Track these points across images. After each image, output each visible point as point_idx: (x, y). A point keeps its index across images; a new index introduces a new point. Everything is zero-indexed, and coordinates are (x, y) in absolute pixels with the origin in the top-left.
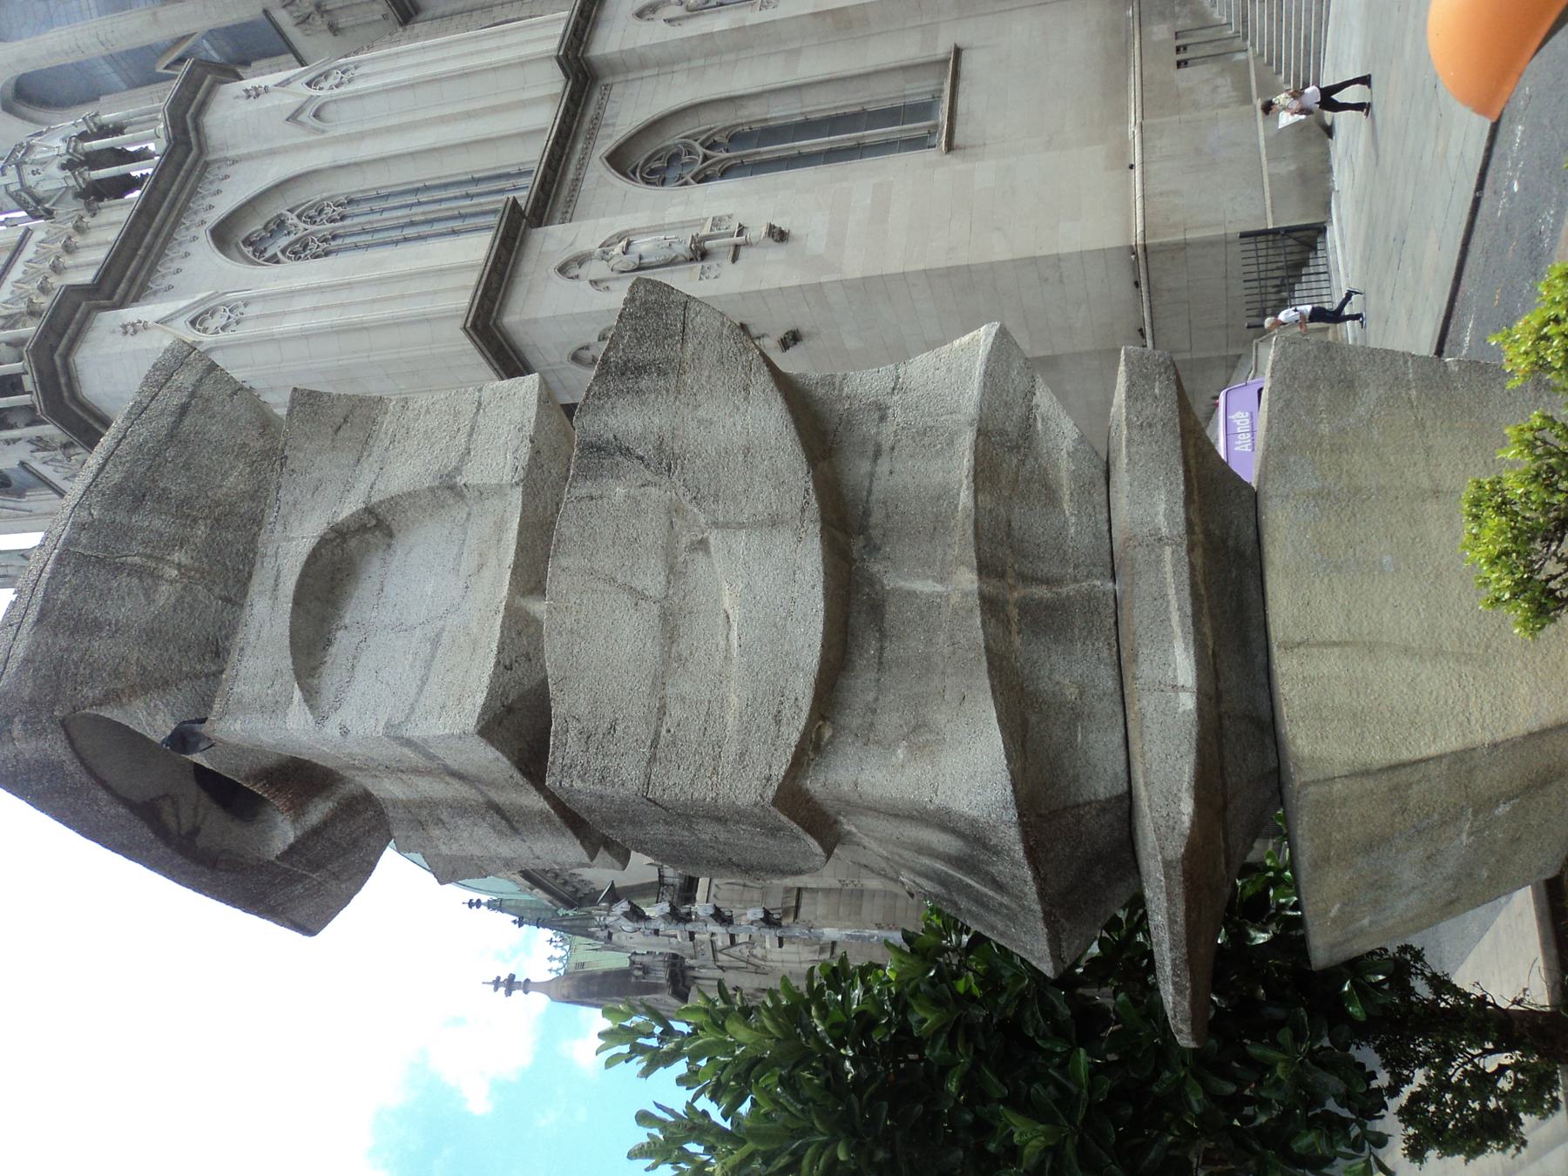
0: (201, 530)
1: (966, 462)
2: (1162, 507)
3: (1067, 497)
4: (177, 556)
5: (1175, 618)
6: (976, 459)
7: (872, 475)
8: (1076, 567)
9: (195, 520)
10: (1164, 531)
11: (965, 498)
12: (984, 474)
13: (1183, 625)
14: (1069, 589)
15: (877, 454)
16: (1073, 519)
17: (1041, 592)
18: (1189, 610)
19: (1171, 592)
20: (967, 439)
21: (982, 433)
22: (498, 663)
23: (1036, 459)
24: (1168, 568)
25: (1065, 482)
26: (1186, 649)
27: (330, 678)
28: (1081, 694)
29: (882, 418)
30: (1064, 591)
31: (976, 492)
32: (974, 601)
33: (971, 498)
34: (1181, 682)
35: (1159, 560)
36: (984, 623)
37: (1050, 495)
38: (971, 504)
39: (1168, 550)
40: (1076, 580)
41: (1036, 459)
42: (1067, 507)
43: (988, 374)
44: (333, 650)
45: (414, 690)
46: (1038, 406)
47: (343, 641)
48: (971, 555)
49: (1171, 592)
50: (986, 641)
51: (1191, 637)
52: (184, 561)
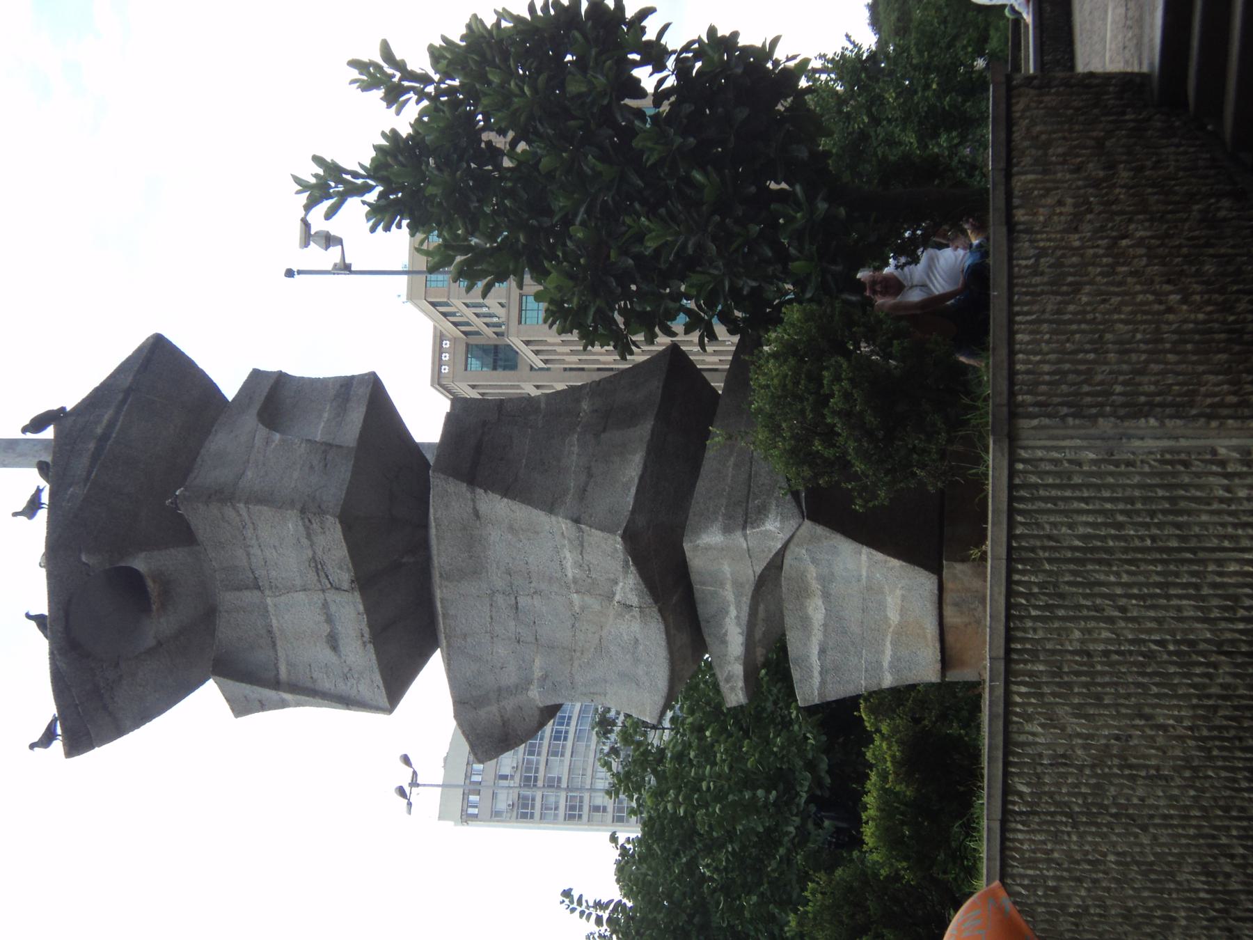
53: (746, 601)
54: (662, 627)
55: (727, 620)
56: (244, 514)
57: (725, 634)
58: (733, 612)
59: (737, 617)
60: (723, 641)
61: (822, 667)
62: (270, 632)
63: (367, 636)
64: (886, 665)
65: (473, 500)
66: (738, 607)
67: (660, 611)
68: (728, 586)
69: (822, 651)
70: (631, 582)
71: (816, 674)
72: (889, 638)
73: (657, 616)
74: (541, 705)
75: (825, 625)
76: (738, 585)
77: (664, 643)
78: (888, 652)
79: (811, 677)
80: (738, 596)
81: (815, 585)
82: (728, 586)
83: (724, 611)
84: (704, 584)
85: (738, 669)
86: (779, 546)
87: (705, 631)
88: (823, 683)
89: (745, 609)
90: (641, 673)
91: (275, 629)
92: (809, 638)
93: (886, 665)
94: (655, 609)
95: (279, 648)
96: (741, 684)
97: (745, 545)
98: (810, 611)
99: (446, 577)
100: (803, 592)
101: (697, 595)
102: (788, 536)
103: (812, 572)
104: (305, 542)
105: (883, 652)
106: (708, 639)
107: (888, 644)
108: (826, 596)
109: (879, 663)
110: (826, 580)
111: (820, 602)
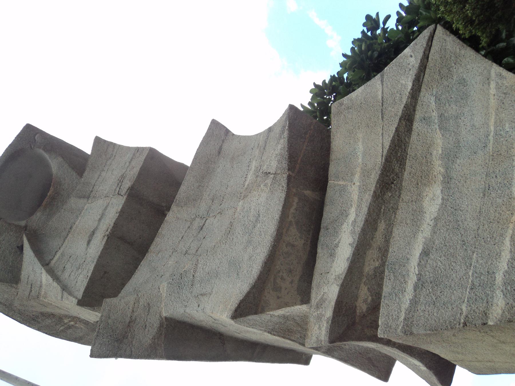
53: (368, 197)
54: (283, 195)
55: (345, 225)
56: (115, 151)
57: (337, 246)
59: (355, 221)
60: (332, 255)
61: (420, 276)
63: (109, 230)
64: (499, 278)
66: (359, 206)
67: (289, 178)
68: (357, 178)
69: (425, 253)
70: (280, 147)
71: (410, 287)
72: (510, 232)
73: (284, 183)
74: (164, 315)
75: (436, 219)
76: (366, 173)
77: (277, 216)
78: (506, 256)
79: (403, 291)
80: (363, 189)
81: (438, 167)
82: (357, 178)
83: (344, 214)
84: (337, 178)
86: (410, 85)
87: (322, 239)
88: (414, 302)
90: (246, 257)
91: (74, 228)
92: (415, 235)
93: (499, 278)
96: (329, 313)
97: (380, 97)
98: (426, 203)
99: (177, 205)
100: (424, 178)
101: (330, 192)
102: (420, 55)
103: (439, 143)
104: (128, 164)
105: (499, 255)
106: (319, 250)
107: (507, 242)
108: (447, 180)
109: (491, 274)
110: (449, 157)
111: (439, 192)
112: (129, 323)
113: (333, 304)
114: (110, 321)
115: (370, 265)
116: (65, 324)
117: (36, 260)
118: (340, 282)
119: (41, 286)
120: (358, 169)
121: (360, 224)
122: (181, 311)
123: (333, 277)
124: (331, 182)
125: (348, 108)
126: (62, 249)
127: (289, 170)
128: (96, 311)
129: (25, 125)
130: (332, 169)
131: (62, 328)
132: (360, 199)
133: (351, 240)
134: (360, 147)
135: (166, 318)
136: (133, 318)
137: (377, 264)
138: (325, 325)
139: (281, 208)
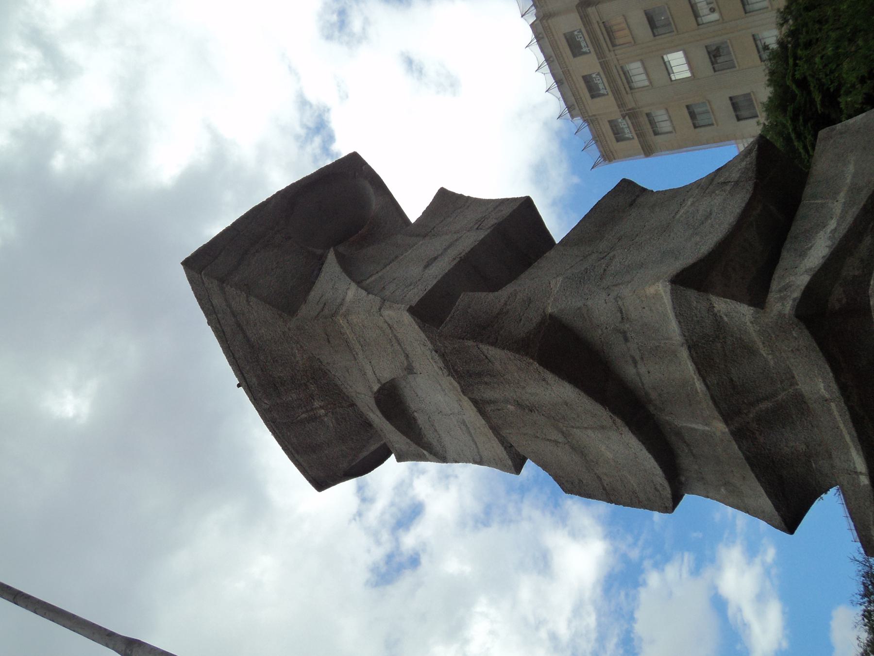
0: (312, 387)
1: (690, 368)
2: (822, 386)
3: (761, 346)
4: (317, 404)
5: (848, 438)
6: (696, 363)
7: (638, 374)
8: (782, 382)
9: (306, 385)
10: (827, 396)
11: (699, 385)
12: (704, 364)
13: (853, 441)
14: (782, 396)
15: (635, 363)
16: (770, 357)
17: (764, 406)
18: (855, 434)
19: (842, 426)
20: (684, 353)
21: (692, 347)
22: (505, 448)
23: (732, 336)
24: (836, 413)
25: (756, 339)
26: (858, 454)
27: (430, 436)
28: (808, 447)
29: (626, 340)
30: (780, 397)
31: (704, 381)
32: (729, 437)
33: (703, 385)
34: (859, 470)
35: (829, 410)
36: (740, 448)
37: (750, 351)
38: (704, 388)
39: (833, 405)
40: (784, 390)
41: (732, 336)
42: (763, 352)
43: (678, 315)
44: (419, 422)
45: (474, 446)
46: (719, 311)
47: (421, 420)
48: (716, 414)
49: (842, 426)
50: (744, 454)
51: (859, 447)
52: (322, 404)
53: (854, 211)
54: (748, 196)
55: (822, 233)
57: (810, 248)
58: (832, 224)
59: (835, 229)
60: (803, 254)
62: (397, 257)
65: (638, 196)
66: (842, 217)
68: (842, 197)
74: (550, 310)
82: (842, 197)
85: (802, 280)
89: (850, 219)
94: (751, 183)
95: (388, 268)
96: (797, 294)
106: (784, 254)
112: (498, 314)
113: (803, 288)
114: (469, 310)
115: (851, 269)
116: (312, 409)
117: (344, 276)
118: (812, 273)
119: (341, 304)
120: (845, 189)
121: (842, 231)
122: (580, 304)
123: (804, 269)
124: (805, 202)
125: (841, 133)
126: (380, 274)
127: (756, 178)
128: (424, 331)
129: (352, 151)
130: (808, 191)
131: (304, 416)
132: (844, 212)
133: (829, 243)
134: (851, 168)
135: (550, 315)
136: (505, 310)
137: (857, 273)
138: (791, 302)
139: (743, 205)
